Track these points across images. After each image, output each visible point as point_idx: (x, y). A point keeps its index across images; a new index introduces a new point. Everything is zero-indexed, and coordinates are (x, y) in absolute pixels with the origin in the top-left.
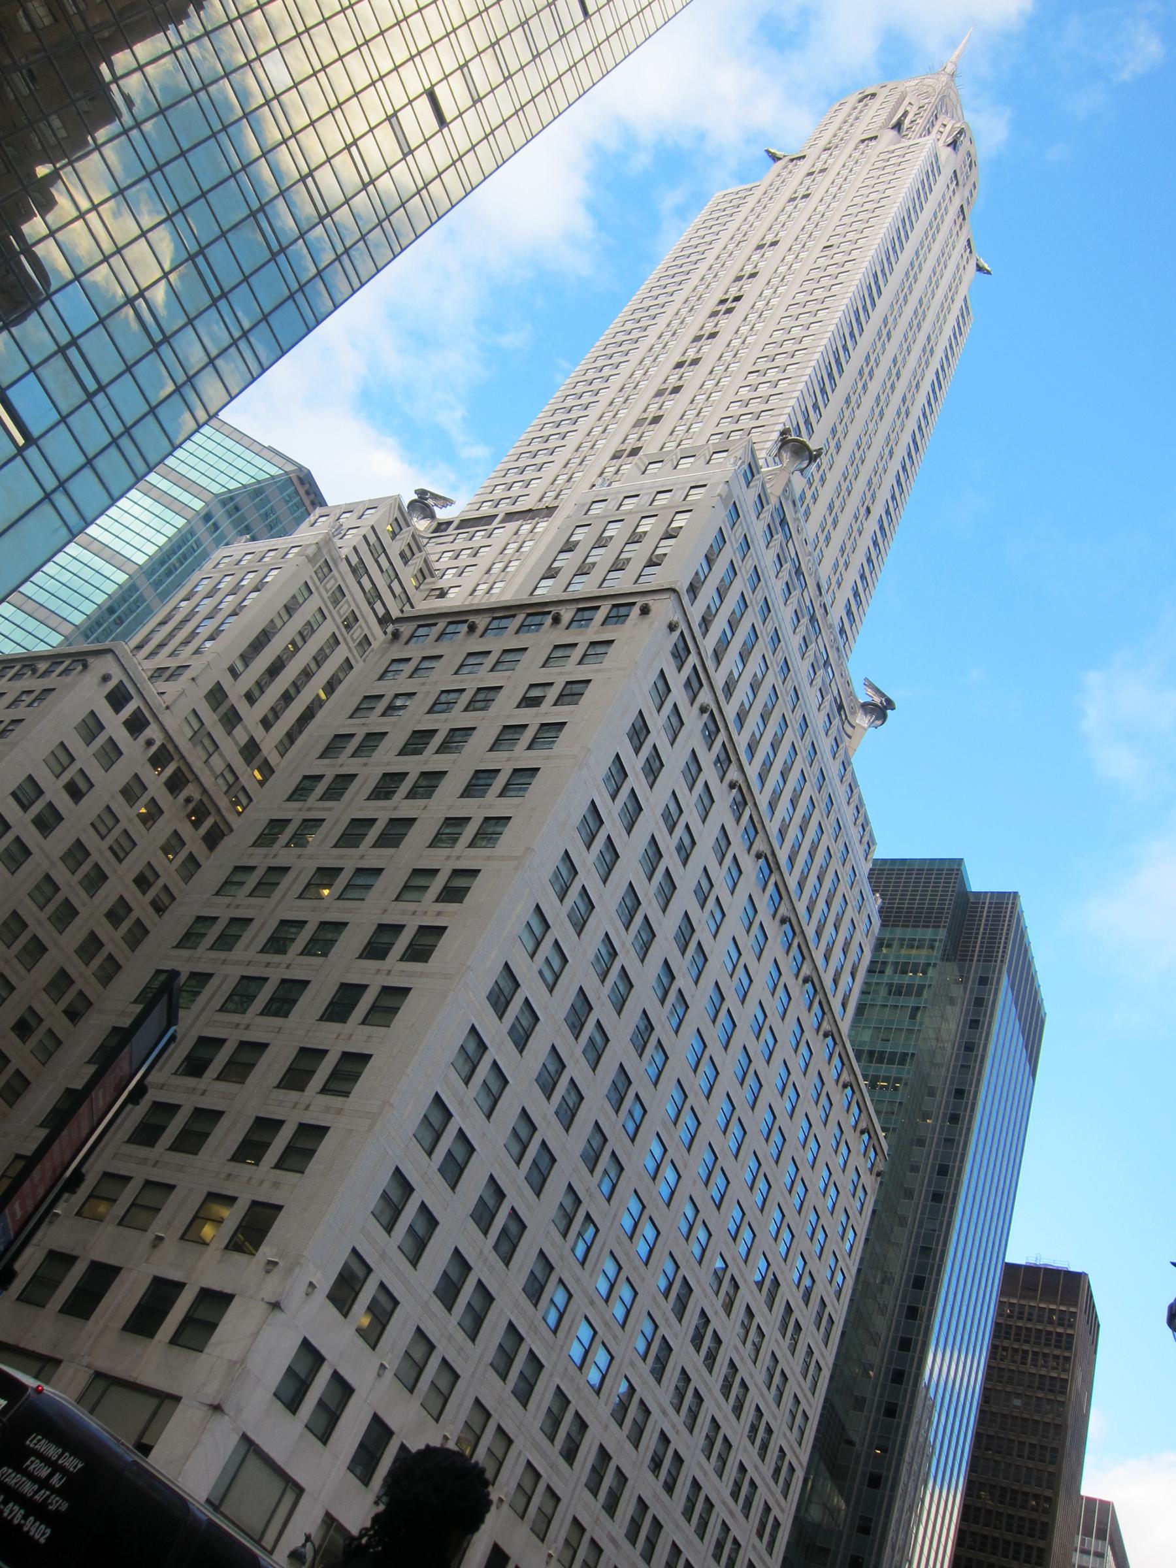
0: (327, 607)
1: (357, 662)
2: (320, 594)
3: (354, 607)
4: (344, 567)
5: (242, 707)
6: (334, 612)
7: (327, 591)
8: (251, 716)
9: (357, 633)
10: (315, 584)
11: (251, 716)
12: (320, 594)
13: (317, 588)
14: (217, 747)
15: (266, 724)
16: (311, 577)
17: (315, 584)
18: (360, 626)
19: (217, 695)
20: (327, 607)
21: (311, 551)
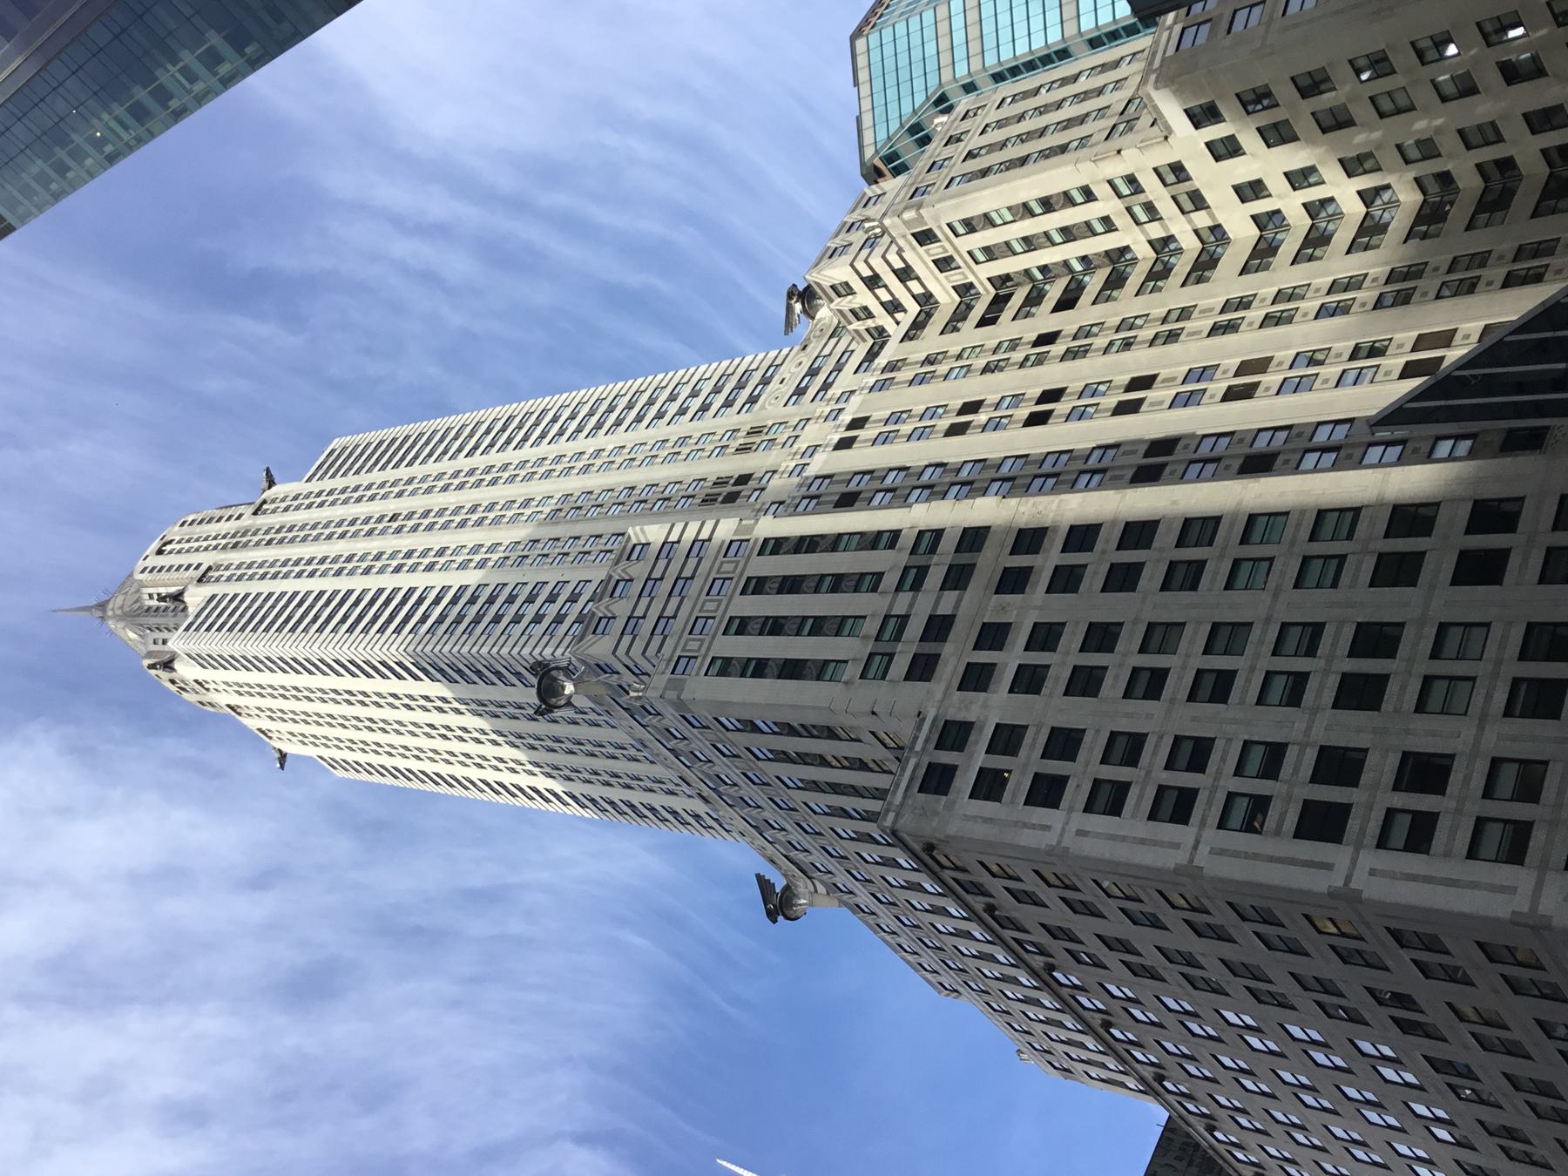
4: (670, 643)
5: (871, 627)
14: (931, 617)
19: (875, 666)
21: (672, 695)
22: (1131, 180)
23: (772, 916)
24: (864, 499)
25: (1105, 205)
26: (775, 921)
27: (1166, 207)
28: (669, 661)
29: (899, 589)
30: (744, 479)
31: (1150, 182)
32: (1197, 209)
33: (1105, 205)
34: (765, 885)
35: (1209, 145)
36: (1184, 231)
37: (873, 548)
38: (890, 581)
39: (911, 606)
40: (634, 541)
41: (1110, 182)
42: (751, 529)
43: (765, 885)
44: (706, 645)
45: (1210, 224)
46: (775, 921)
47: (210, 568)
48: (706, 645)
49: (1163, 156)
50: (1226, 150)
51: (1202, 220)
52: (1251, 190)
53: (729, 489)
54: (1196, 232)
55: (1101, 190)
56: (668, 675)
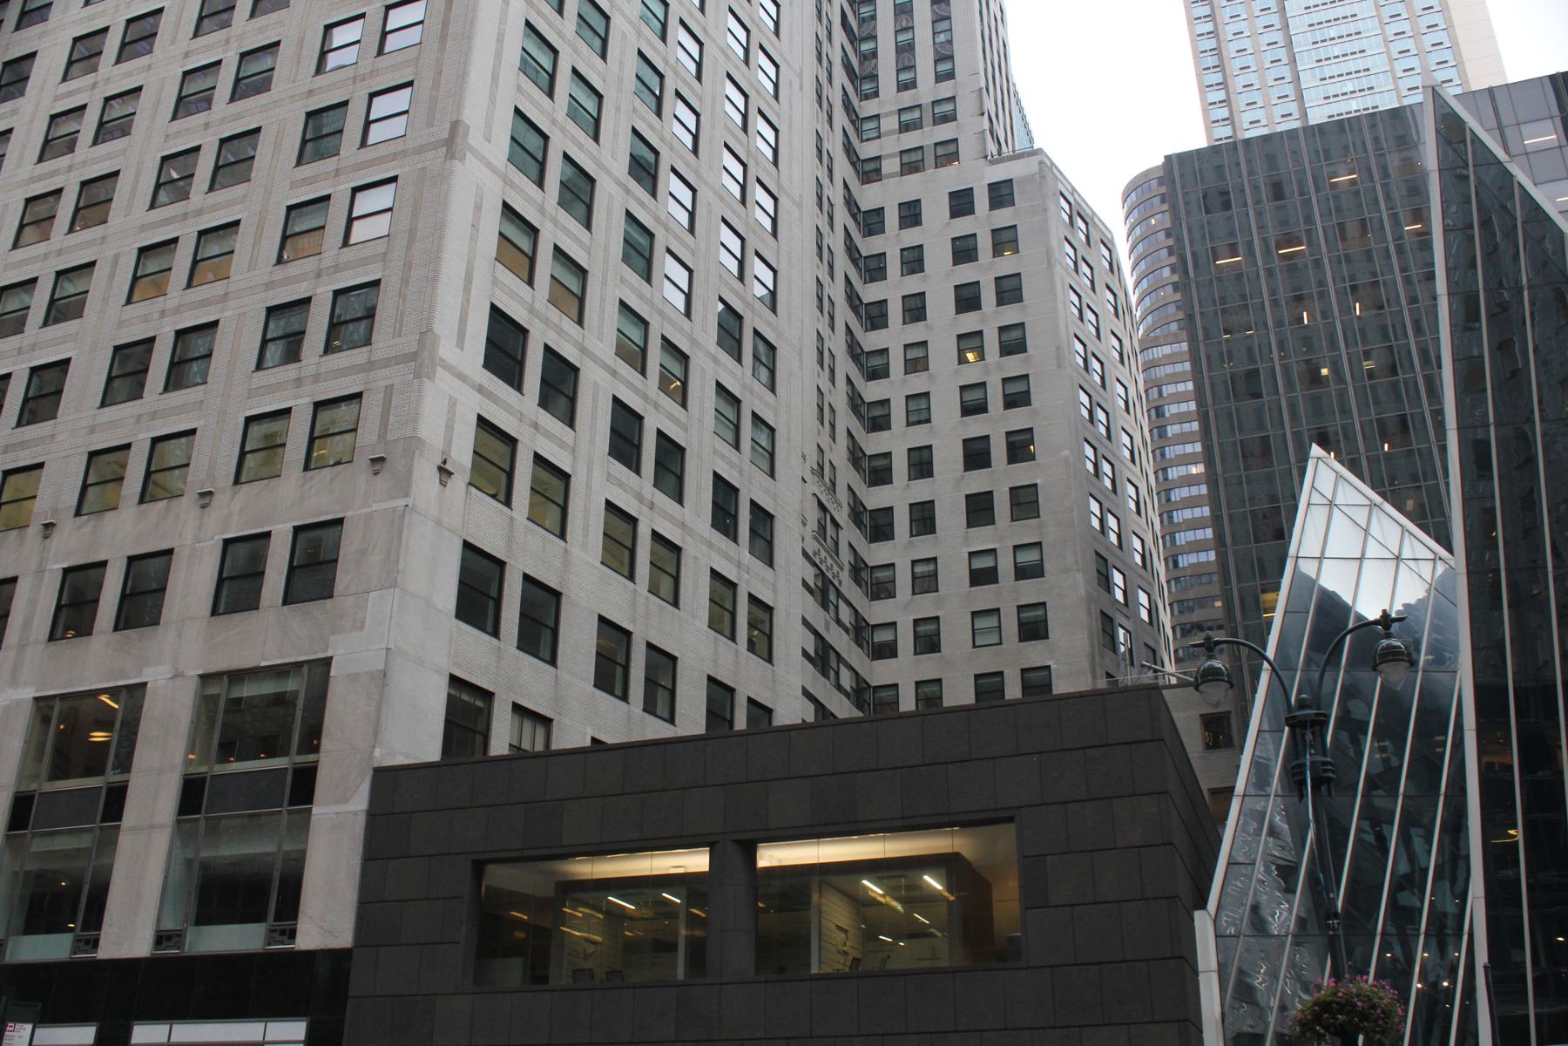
22: (949, 118)
25: (927, 90)
27: (911, 140)
31: (945, 132)
32: (902, 165)
33: (927, 90)
35: (969, 192)
36: (888, 146)
41: (953, 98)
45: (884, 171)
49: (967, 148)
50: (961, 203)
51: (890, 166)
52: (911, 214)
54: (879, 158)
55: (945, 89)
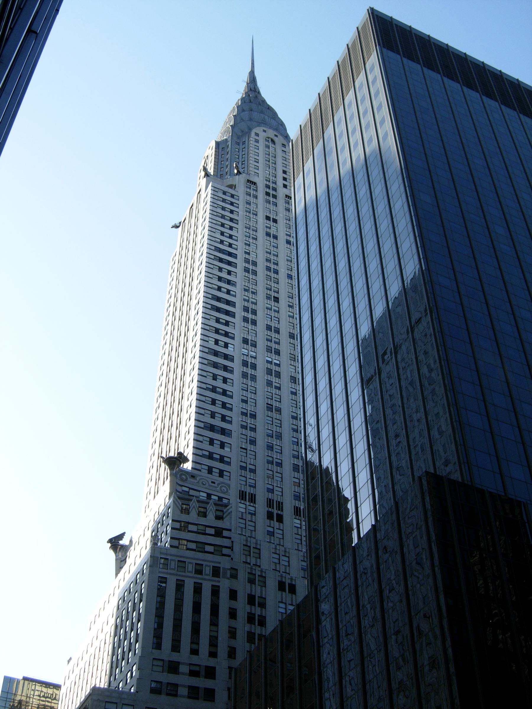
0: (180, 575)
1: (219, 582)
2: (171, 574)
3: (195, 562)
6: (187, 574)
7: (174, 569)
8: (184, 655)
9: (208, 570)
10: (164, 573)
11: (184, 655)
12: (171, 574)
13: (167, 573)
15: (195, 652)
16: (159, 572)
17: (164, 573)
18: (206, 566)
20: (180, 575)
23: (110, 541)
24: (251, 609)
26: (108, 542)
28: (166, 554)
29: (190, 664)
30: (280, 519)
34: (121, 536)
37: (210, 645)
38: (195, 659)
39: (183, 674)
40: (225, 510)
42: (225, 576)
43: (121, 536)
44: (173, 572)
46: (108, 542)
47: (255, 184)
48: (173, 572)
53: (275, 512)
56: (159, 556)
